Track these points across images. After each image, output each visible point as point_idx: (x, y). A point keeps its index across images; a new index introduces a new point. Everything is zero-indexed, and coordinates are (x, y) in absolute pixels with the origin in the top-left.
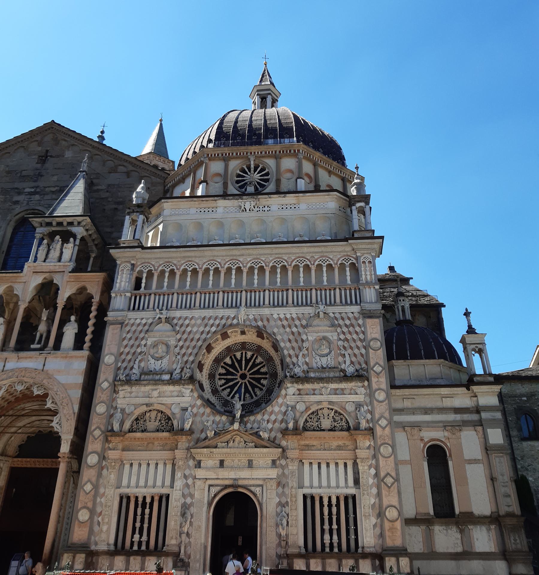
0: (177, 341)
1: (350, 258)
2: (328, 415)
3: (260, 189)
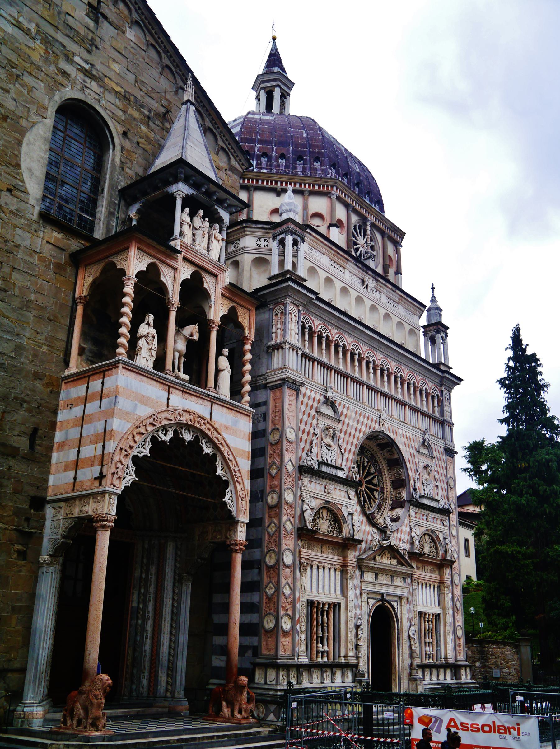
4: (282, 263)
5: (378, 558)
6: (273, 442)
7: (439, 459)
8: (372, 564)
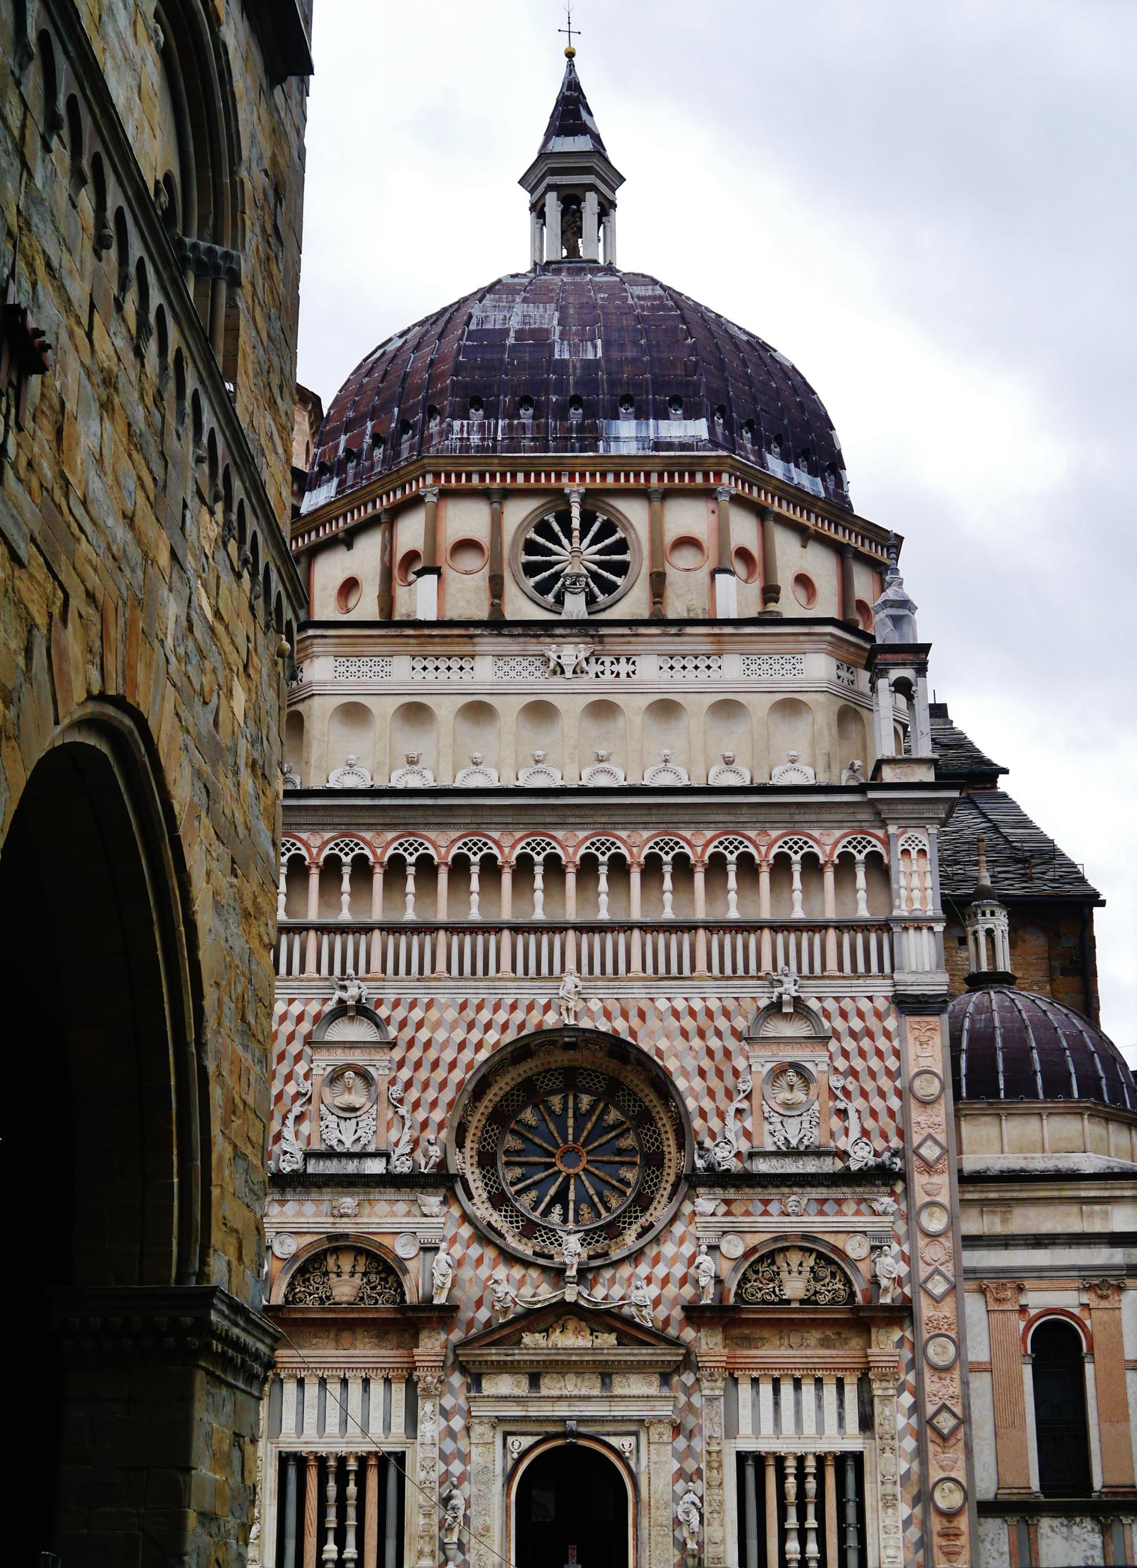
0: (395, 1067)
1: (869, 838)
2: (801, 1265)
3: (601, 598)
5: (527, 1339)
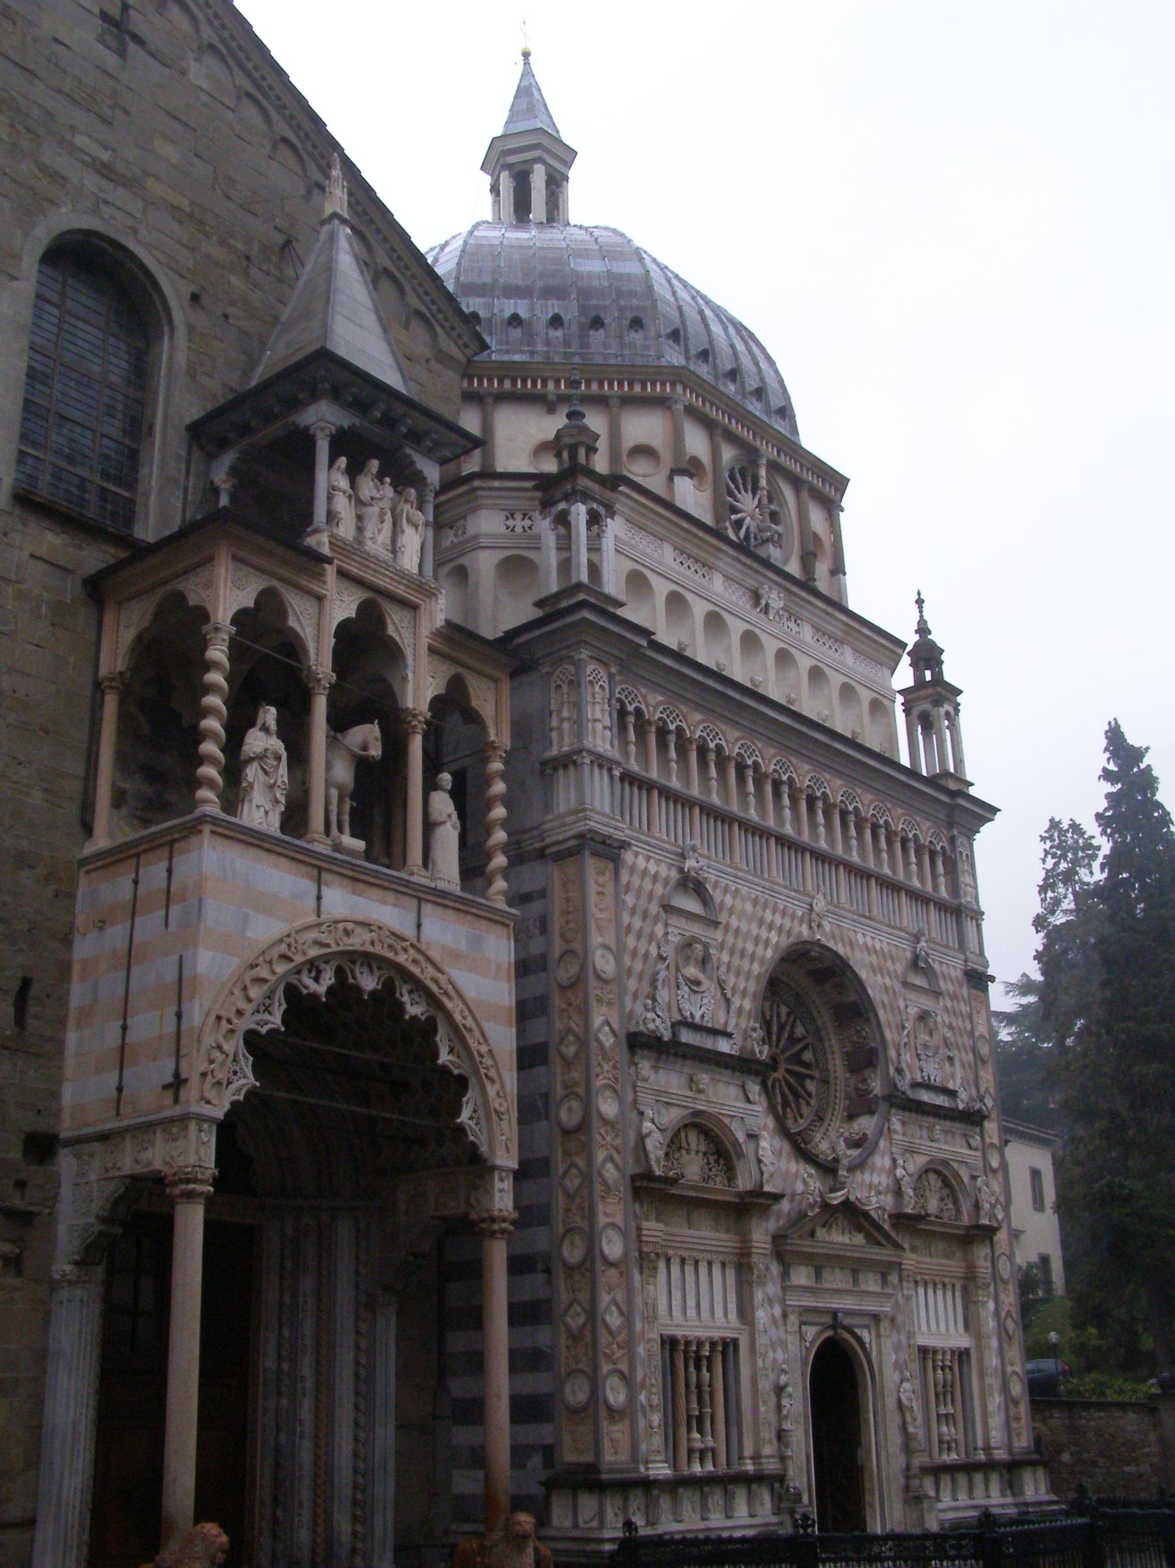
4: (565, 566)
5: (821, 1233)
6: (565, 982)
7: (953, 997)
8: (806, 1246)
